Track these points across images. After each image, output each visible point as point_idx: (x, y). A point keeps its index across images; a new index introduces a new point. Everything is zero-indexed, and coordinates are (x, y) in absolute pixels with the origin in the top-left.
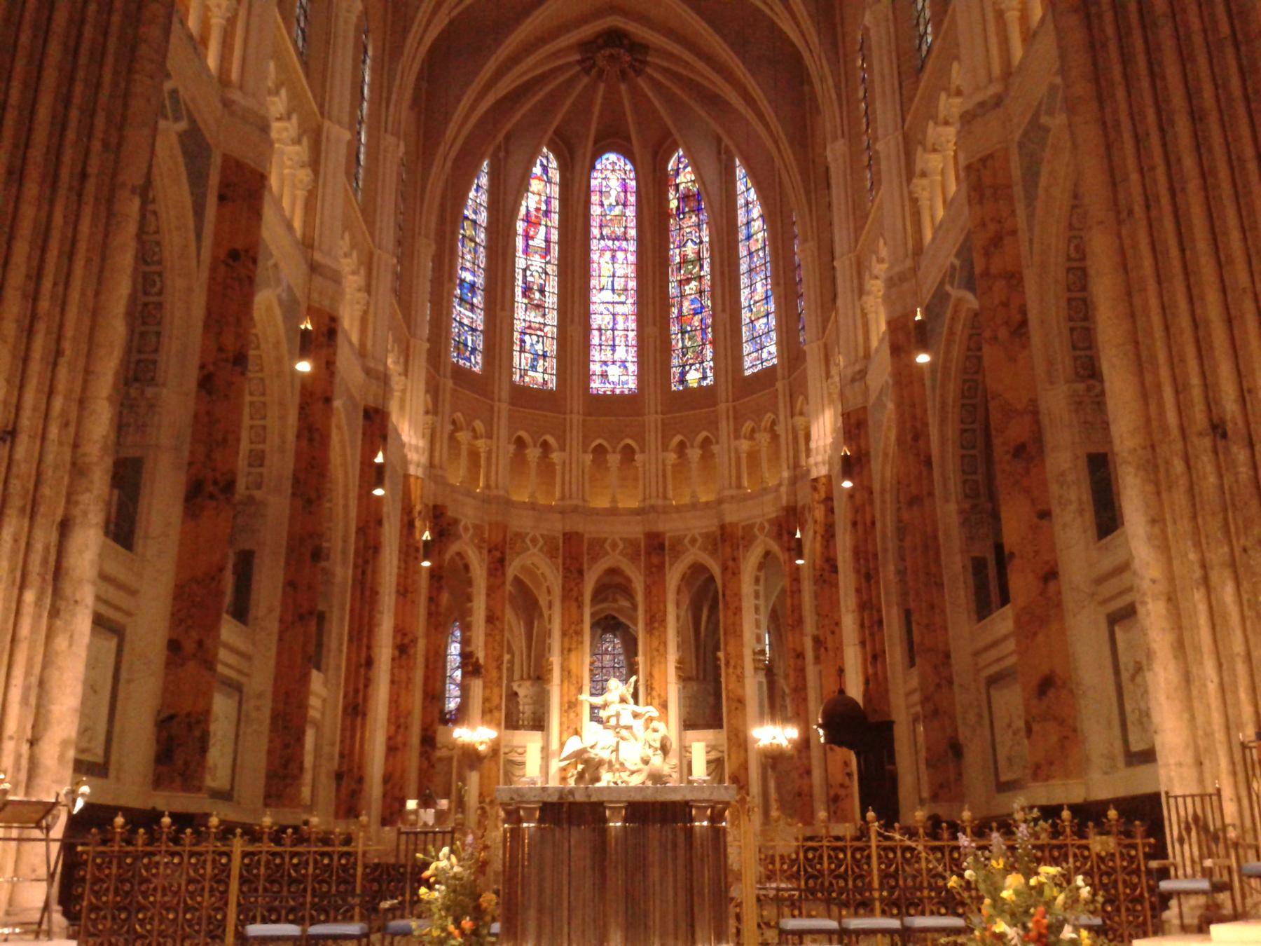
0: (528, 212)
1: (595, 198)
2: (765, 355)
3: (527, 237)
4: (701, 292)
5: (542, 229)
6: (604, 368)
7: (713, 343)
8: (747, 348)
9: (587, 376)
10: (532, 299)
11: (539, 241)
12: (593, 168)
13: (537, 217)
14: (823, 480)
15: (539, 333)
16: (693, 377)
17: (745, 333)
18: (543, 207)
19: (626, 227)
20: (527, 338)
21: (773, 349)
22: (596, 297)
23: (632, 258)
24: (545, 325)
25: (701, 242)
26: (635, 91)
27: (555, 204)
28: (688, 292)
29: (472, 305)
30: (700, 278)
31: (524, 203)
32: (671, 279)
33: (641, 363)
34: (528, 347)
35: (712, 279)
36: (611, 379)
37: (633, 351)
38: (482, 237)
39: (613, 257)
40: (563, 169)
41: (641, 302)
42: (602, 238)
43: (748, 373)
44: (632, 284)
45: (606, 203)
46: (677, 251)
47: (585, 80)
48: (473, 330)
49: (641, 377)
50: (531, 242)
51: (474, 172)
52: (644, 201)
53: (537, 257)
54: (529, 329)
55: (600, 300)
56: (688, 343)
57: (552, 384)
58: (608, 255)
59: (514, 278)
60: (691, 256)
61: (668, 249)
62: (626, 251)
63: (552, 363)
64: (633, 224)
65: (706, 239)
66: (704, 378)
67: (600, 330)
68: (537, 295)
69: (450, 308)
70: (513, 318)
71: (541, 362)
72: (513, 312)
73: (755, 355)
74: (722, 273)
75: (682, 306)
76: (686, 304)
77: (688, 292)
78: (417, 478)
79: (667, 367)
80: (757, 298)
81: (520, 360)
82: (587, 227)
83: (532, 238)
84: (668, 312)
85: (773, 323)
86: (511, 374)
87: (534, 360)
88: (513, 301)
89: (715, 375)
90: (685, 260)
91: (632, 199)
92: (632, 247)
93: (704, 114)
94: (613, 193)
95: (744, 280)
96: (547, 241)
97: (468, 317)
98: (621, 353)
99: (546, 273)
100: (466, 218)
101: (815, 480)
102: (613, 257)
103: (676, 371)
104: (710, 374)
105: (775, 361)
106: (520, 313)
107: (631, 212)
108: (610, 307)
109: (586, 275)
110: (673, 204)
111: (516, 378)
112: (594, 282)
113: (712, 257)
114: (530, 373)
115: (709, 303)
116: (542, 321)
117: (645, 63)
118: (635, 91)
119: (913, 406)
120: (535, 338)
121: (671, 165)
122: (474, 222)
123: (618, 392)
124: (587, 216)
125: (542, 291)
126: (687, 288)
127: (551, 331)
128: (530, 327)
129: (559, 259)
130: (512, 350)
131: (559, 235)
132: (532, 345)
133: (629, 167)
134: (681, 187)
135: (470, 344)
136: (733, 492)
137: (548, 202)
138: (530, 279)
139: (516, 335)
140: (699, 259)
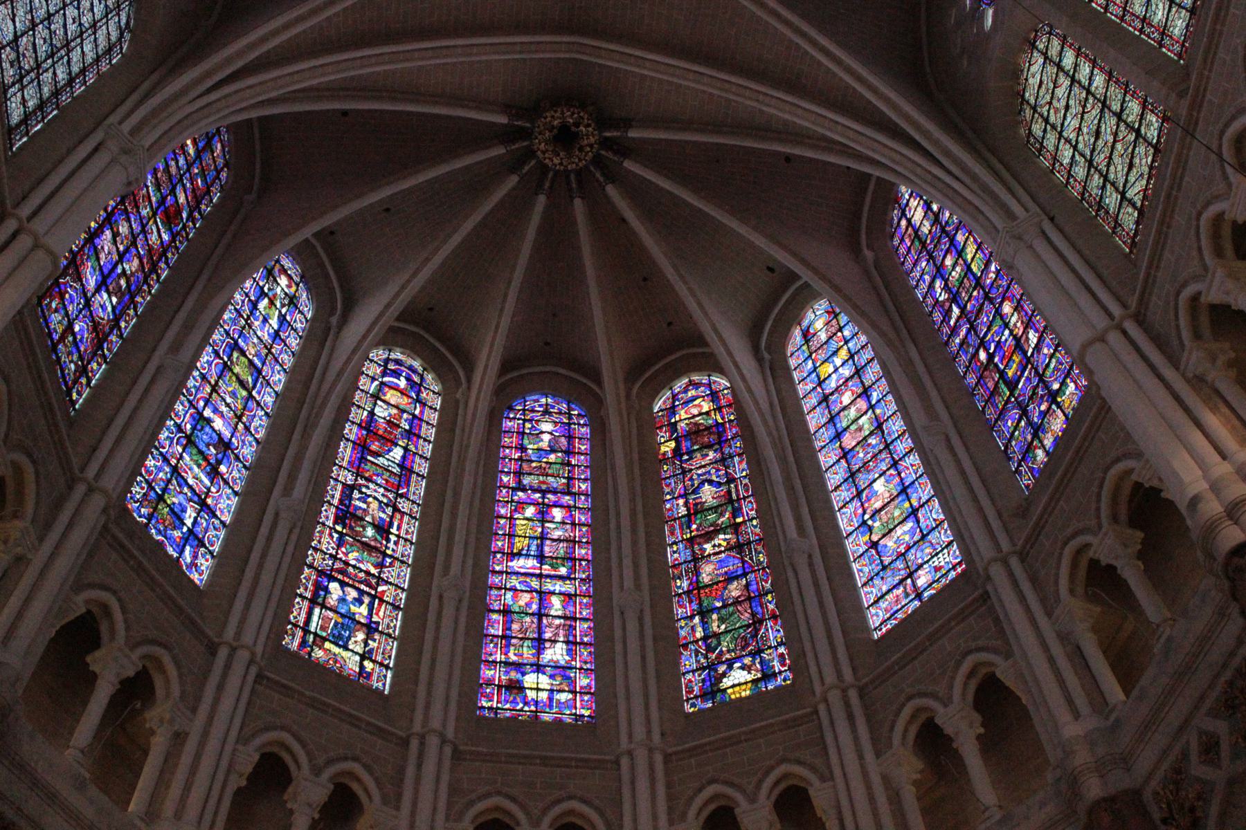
6: (514, 675)
20: (334, 587)
24: (381, 581)
34: (332, 601)
39: (543, 515)
57: (383, 681)
58: (530, 511)
68: (370, 532)
71: (361, 636)
90: (696, 510)
102: (543, 515)
108: (535, 584)
114: (327, 645)
116: (373, 571)
117: (624, 149)
125: (383, 529)
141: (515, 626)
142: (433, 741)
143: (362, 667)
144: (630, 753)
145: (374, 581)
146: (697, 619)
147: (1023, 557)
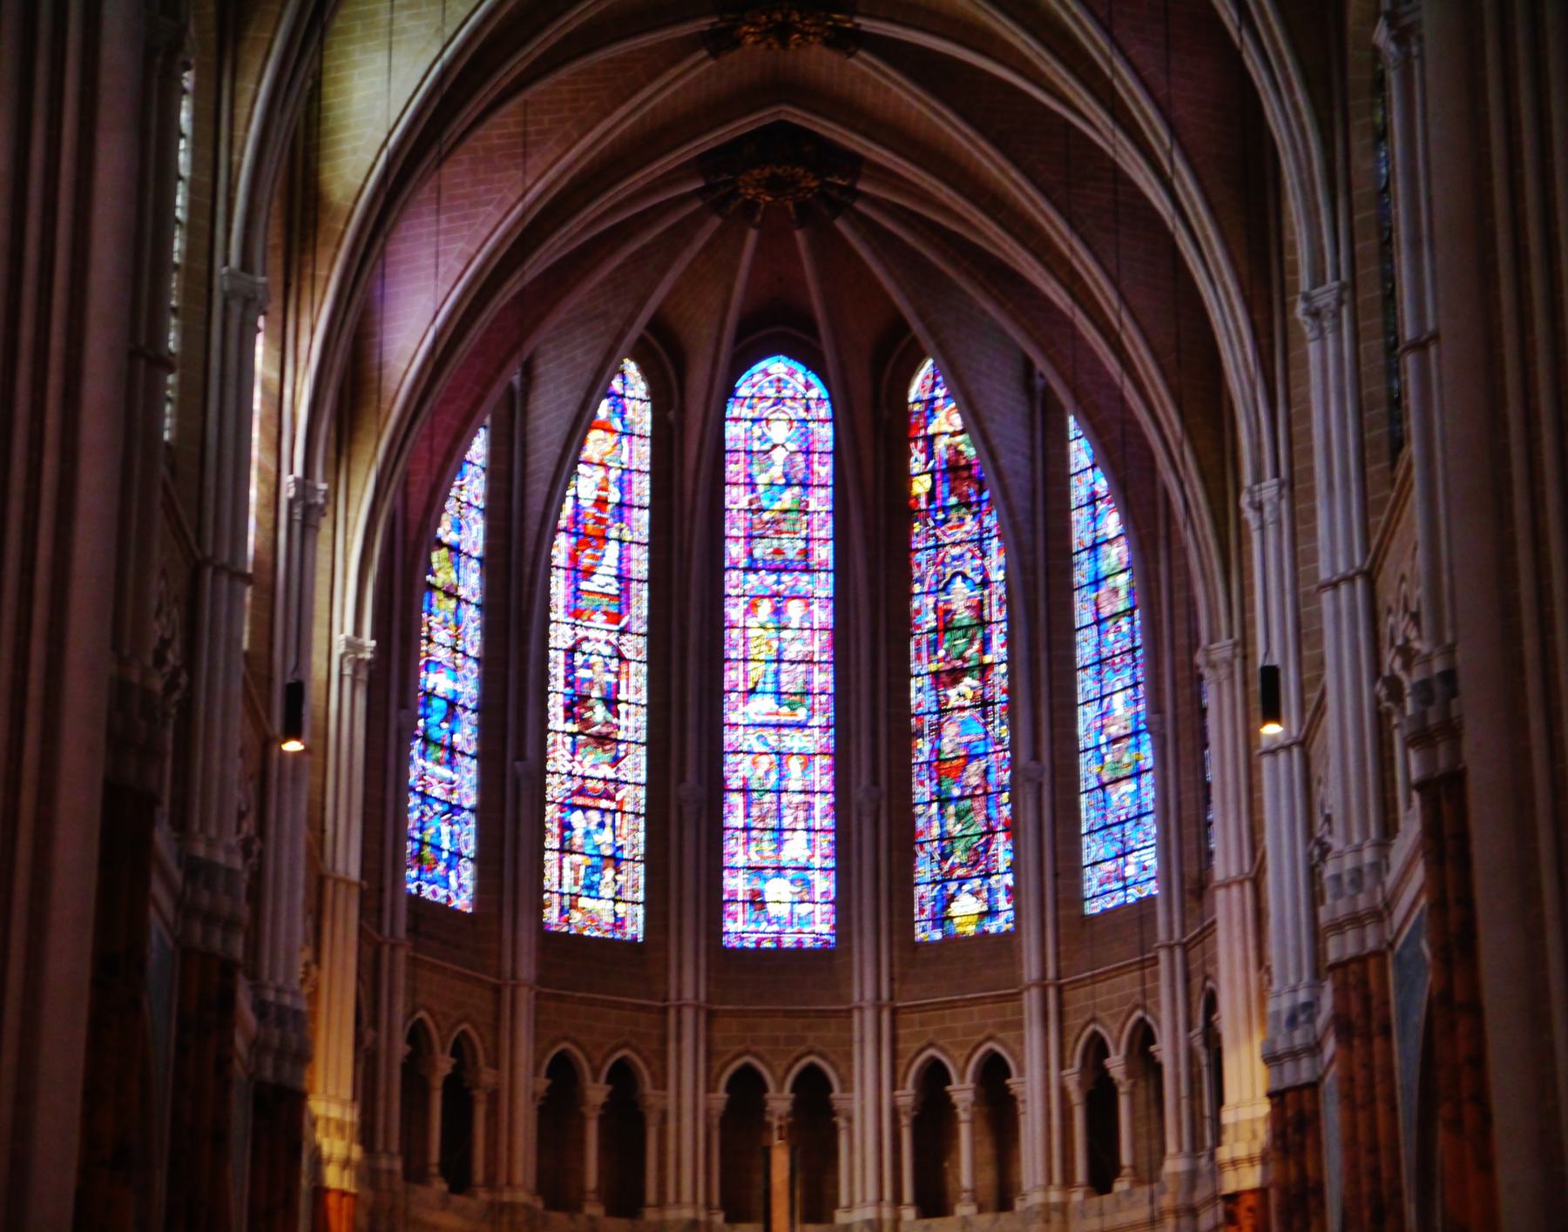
0: (577, 506)
1: (733, 470)
2: (1130, 871)
3: (579, 572)
4: (983, 704)
5: (612, 550)
7: (1011, 829)
8: (1093, 848)
9: (714, 904)
10: (587, 723)
11: (603, 581)
12: (731, 392)
13: (599, 521)
14: (1250, 1201)
15: (604, 804)
16: (965, 907)
17: (1088, 815)
18: (614, 496)
19: (807, 540)
21: (1150, 858)
22: (737, 712)
23: (823, 615)
25: (986, 583)
26: (831, 250)
27: (642, 489)
28: (953, 703)
29: (452, 749)
30: (985, 669)
31: (571, 492)
32: (915, 667)
33: (843, 871)
35: (1011, 673)
36: (772, 909)
37: (824, 842)
38: (471, 582)
39: (777, 612)
40: (660, 398)
41: (842, 725)
42: (752, 568)
43: (1092, 908)
44: (823, 678)
45: (762, 479)
46: (931, 600)
47: (715, 222)
48: (455, 809)
49: (842, 905)
50: (584, 585)
51: (460, 441)
52: (849, 474)
53: (599, 619)
54: (582, 796)
55: (746, 716)
56: (954, 828)
57: (635, 929)
58: (765, 607)
59: (544, 676)
60: (963, 616)
61: (911, 595)
62: (807, 599)
63: (635, 875)
64: (826, 531)
65: (997, 576)
66: (992, 913)
67: (745, 790)
68: (599, 713)
69: (404, 761)
70: (544, 772)
71: (609, 873)
72: (543, 757)
73: (1110, 866)
74: (1033, 664)
75: (939, 737)
76: (950, 731)
77: (953, 703)
78: (343, 1194)
79: (906, 882)
80: (1114, 730)
81: (561, 874)
82: (717, 539)
83: (589, 573)
84: (908, 752)
85: (1149, 797)
86: (541, 906)
87: (593, 869)
88: (544, 730)
89: (1017, 909)
90: (946, 621)
91: (824, 471)
92: (823, 586)
93: (989, 307)
94: (779, 456)
95: (1086, 684)
96: (623, 578)
97: (445, 780)
98: (796, 848)
99: (622, 658)
100: (440, 544)
101: (1233, 1198)
103: (924, 892)
104: (1003, 904)
105: (1152, 888)
106: (559, 758)
107: (820, 501)
108: (771, 736)
109: (715, 660)
110: (921, 485)
111: (552, 915)
112: (733, 676)
113: (1009, 620)
115: (1004, 731)
116: (610, 773)
118: (831, 250)
119: (1374, 1149)
120: (595, 816)
121: (916, 390)
122: (455, 549)
123: (788, 941)
124: (717, 511)
125: (611, 702)
126: (952, 693)
127: (634, 797)
128: (581, 792)
129: (652, 620)
130: (543, 850)
131: (652, 562)
132: (587, 834)
133: (819, 390)
134: (941, 445)
135: (446, 845)
136: (1055, 1196)
137: (624, 485)
138: (583, 673)
139: (551, 811)
140: (983, 623)
141: (755, 811)
142: (688, 1015)
143: (615, 914)
144: (861, 1009)
145: (611, 787)
146: (935, 806)
147: (1186, 948)
